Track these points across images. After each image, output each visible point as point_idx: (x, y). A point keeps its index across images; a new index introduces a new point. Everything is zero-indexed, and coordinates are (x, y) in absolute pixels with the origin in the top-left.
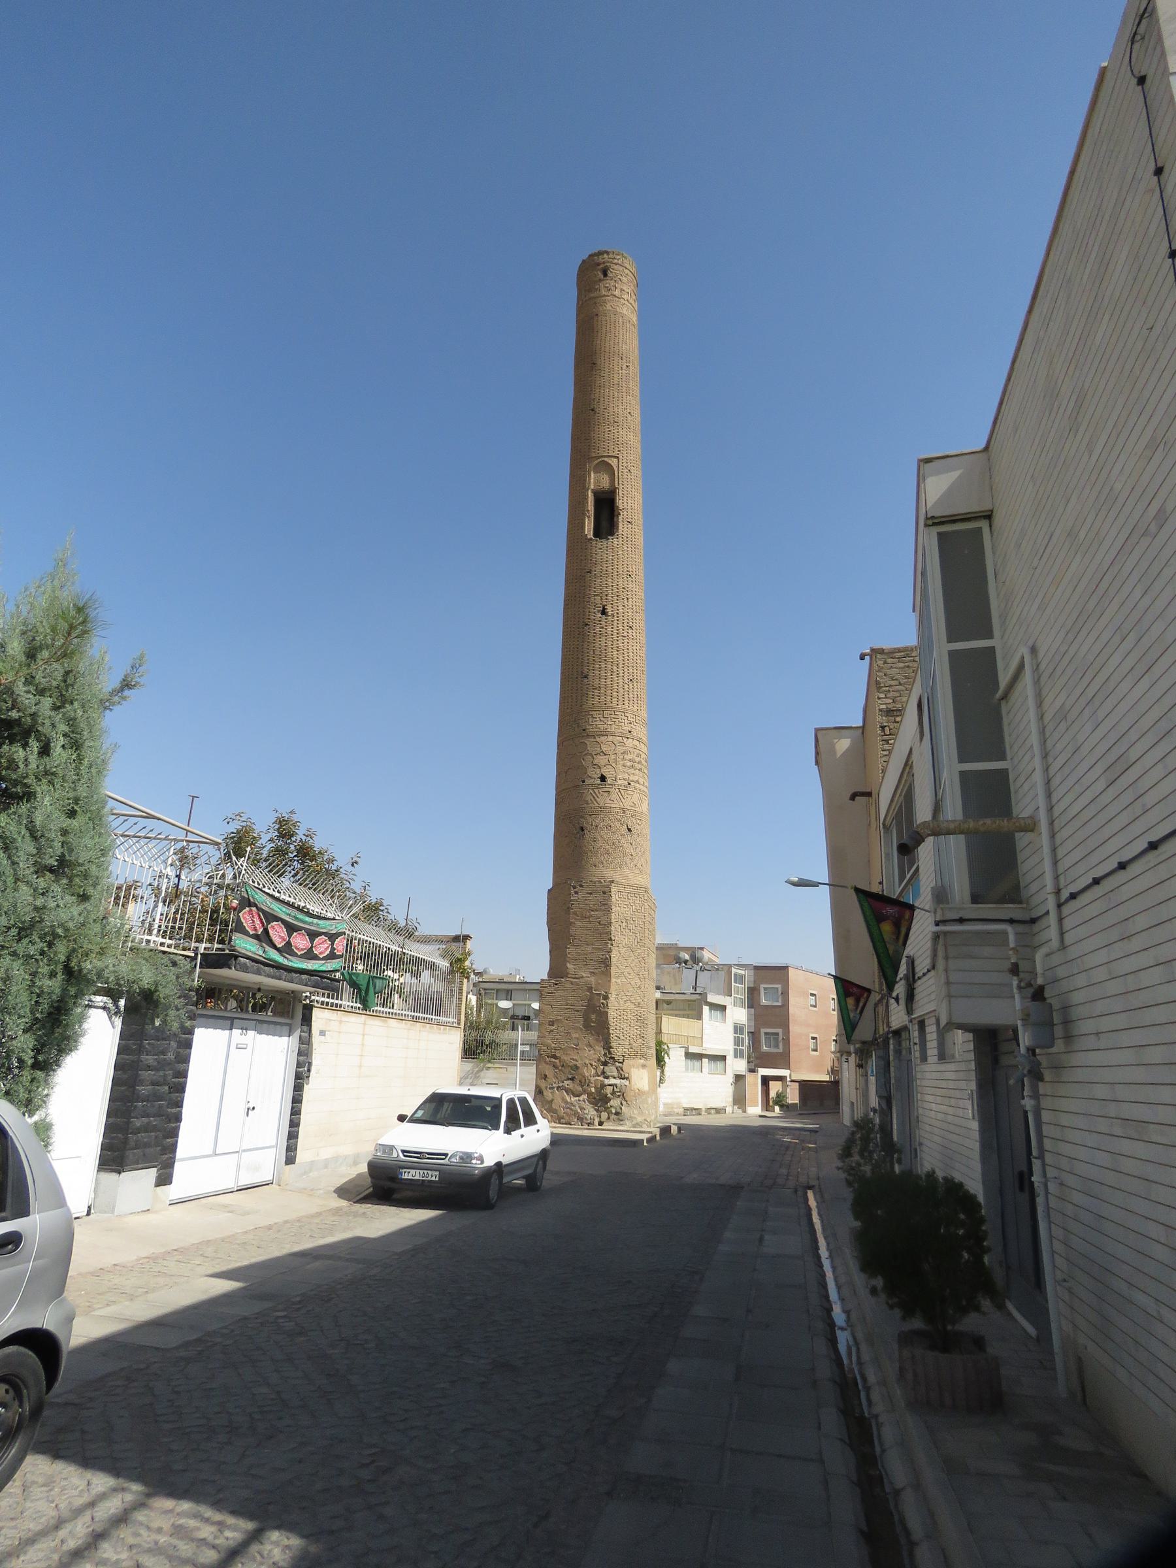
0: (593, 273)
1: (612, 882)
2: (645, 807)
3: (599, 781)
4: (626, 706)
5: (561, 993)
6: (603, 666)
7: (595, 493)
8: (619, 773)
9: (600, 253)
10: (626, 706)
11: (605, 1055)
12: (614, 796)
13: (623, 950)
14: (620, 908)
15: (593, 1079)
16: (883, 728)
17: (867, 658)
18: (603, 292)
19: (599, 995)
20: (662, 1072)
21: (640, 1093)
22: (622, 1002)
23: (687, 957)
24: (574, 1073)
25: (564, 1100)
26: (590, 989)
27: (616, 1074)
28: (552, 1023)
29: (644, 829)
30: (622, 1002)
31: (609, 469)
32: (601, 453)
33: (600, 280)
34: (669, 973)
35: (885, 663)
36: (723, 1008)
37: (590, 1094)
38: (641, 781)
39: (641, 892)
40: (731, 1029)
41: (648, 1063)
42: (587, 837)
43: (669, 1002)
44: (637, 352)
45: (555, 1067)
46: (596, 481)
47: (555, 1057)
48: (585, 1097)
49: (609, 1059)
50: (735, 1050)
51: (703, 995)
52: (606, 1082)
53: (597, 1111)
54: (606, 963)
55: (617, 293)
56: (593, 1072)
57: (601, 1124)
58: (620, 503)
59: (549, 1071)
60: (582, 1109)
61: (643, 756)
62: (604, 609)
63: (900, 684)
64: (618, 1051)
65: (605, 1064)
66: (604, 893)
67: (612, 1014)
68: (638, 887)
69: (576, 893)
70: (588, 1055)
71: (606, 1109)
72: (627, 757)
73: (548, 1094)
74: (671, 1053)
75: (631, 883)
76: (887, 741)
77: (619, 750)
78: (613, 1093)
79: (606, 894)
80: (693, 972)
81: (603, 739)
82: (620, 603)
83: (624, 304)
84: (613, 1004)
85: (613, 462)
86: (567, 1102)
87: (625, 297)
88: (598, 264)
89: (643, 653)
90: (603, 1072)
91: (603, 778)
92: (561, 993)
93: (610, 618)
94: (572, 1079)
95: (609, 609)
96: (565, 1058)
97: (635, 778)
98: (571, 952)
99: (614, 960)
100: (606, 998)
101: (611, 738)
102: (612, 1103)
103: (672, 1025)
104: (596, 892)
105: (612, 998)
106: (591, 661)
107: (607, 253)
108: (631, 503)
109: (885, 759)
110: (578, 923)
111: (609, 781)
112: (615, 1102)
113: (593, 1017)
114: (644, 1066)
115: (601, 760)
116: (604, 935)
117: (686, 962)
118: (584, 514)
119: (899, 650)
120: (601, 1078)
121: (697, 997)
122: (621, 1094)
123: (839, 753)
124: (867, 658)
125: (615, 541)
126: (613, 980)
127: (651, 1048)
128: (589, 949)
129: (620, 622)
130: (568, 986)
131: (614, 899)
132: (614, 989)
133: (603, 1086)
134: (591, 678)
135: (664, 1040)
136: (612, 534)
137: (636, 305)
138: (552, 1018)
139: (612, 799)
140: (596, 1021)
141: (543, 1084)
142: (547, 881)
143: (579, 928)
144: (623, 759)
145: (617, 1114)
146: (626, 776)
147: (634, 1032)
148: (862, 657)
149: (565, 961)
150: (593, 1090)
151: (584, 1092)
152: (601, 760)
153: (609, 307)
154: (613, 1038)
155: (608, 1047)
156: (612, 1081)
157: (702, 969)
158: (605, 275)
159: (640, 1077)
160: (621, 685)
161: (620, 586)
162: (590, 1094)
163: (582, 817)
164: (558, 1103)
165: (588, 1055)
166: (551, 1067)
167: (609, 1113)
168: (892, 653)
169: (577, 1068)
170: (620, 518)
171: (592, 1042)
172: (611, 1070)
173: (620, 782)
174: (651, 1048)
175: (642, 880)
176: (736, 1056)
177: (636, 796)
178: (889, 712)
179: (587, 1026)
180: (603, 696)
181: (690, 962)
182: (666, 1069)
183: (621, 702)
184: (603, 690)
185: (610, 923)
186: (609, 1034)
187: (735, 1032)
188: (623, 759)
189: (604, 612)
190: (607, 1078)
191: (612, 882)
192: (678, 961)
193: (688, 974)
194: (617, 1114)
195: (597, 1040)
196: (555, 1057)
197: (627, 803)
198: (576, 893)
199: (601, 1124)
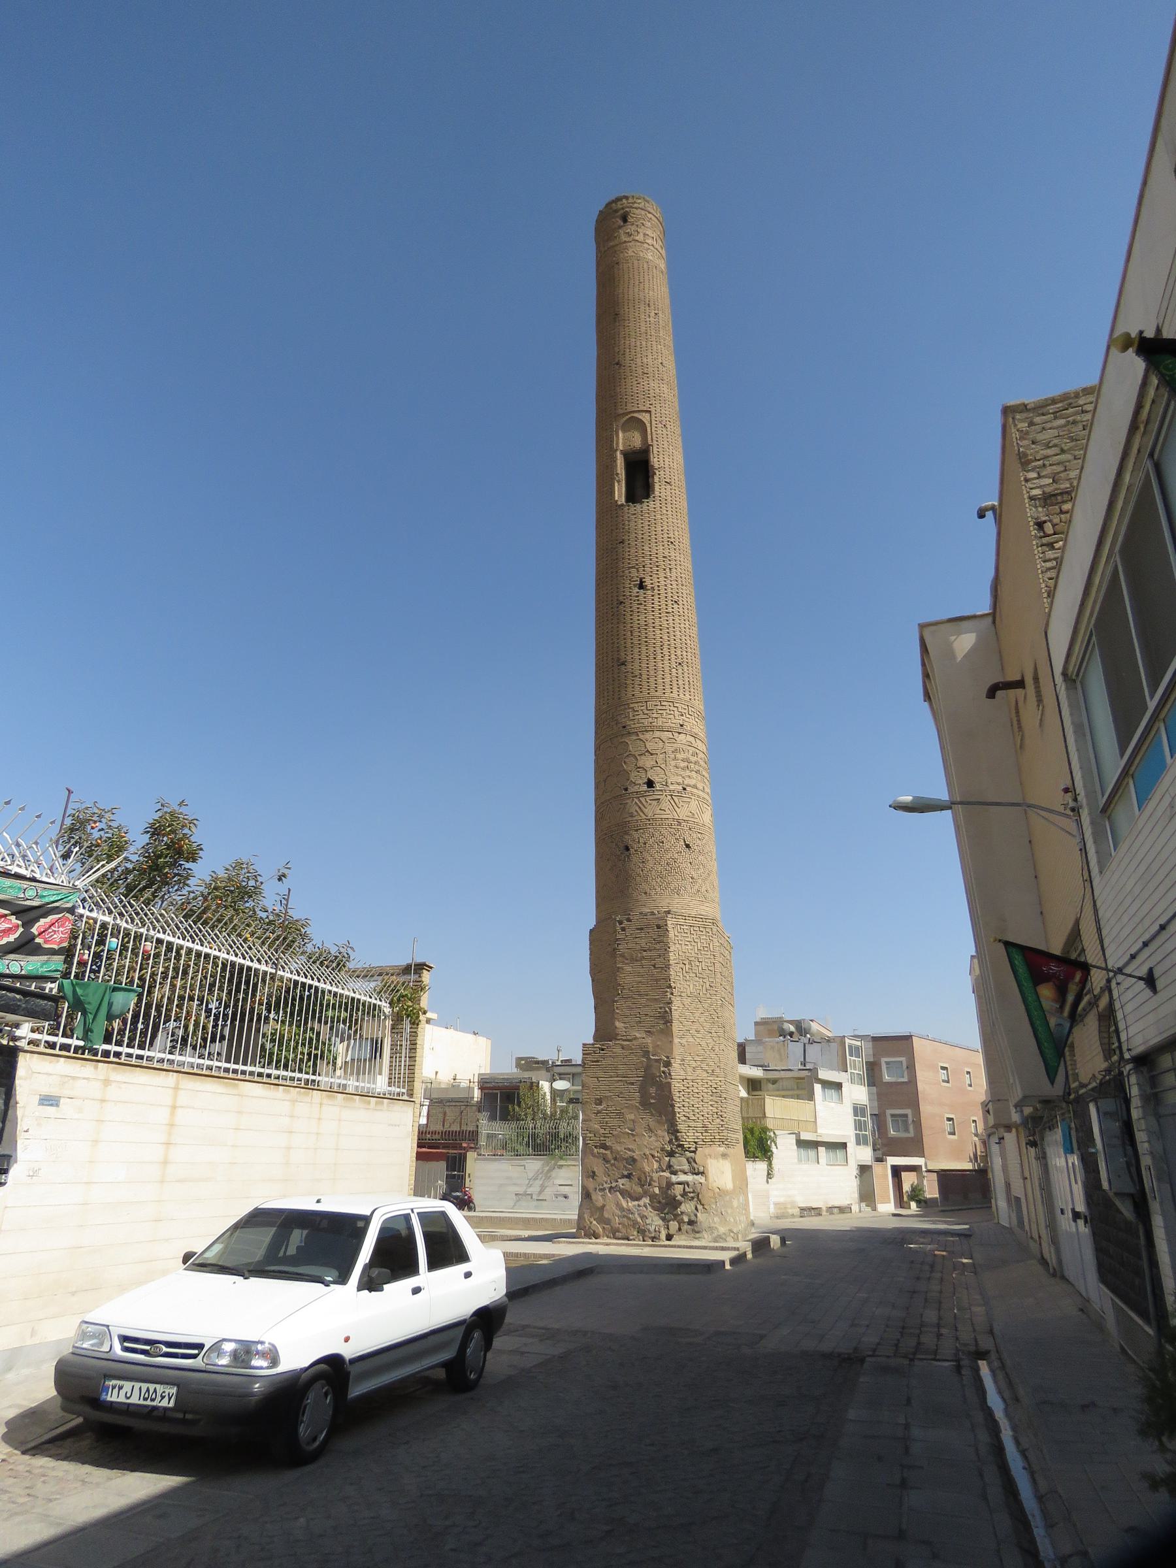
0: (613, 221)
1: (669, 912)
2: (707, 818)
3: (645, 788)
4: (675, 695)
5: (609, 1061)
6: (644, 648)
7: (626, 455)
8: (670, 776)
9: (618, 199)
10: (675, 695)
11: (670, 1142)
12: (665, 804)
13: (687, 1001)
14: (680, 944)
15: (655, 1176)
16: (1040, 525)
17: (989, 514)
18: (624, 238)
19: (657, 1061)
20: (770, 1165)
21: (722, 1192)
22: (689, 1070)
23: (792, 1028)
24: (629, 1167)
25: (618, 1205)
26: (646, 1053)
27: (686, 1167)
28: (599, 1102)
29: (708, 844)
30: (689, 1070)
31: (641, 427)
32: (630, 408)
33: (620, 227)
34: (772, 1048)
35: (1031, 424)
36: (838, 1086)
37: (653, 1197)
38: (700, 786)
39: (705, 923)
40: (851, 1111)
41: (730, 1151)
42: (635, 859)
43: (774, 1082)
44: (667, 301)
45: (606, 1160)
46: (624, 440)
47: (604, 1146)
48: (646, 1200)
49: (676, 1147)
50: (857, 1136)
51: (814, 1071)
52: (674, 1178)
53: (663, 1219)
54: (666, 1019)
55: (640, 237)
56: (656, 1165)
57: (669, 1237)
58: (655, 461)
59: (599, 1168)
60: (643, 1217)
61: (701, 755)
62: (642, 582)
63: (1063, 451)
64: (688, 1136)
65: (671, 1154)
66: (659, 927)
67: (676, 1086)
68: (703, 918)
69: (623, 929)
70: (648, 1143)
71: (676, 1216)
72: (680, 756)
73: (598, 1198)
74: (778, 1141)
75: (693, 913)
76: (1051, 546)
77: (669, 748)
78: (684, 1194)
79: (661, 927)
80: (800, 1046)
81: (648, 736)
82: (662, 574)
83: (649, 248)
84: (680, 1075)
85: (645, 418)
86: (622, 1209)
87: (650, 241)
88: (616, 211)
89: (694, 631)
90: (669, 1166)
91: (650, 784)
92: (609, 1061)
93: (649, 592)
94: (629, 1176)
95: (648, 582)
96: (618, 1148)
97: (693, 782)
98: (621, 1006)
99: (675, 1014)
100: (668, 1064)
101: (657, 734)
102: (683, 1208)
103: (776, 1108)
104: (648, 926)
105: (676, 1065)
106: (629, 645)
107: (627, 198)
108: (669, 461)
109: (1052, 574)
110: (628, 968)
111: (658, 786)
112: (687, 1207)
113: (652, 1090)
114: (724, 1156)
115: (646, 761)
116: (661, 983)
117: (791, 1034)
118: (613, 479)
119: (1054, 401)
120: (667, 1174)
121: (806, 1073)
122: (694, 1195)
123: (960, 655)
124: (989, 514)
125: (649, 505)
126: (676, 1040)
127: (735, 1131)
128: (643, 1001)
129: (663, 596)
130: (618, 1050)
131: (671, 934)
132: (677, 1051)
133: (670, 1185)
134: (629, 666)
135: (770, 1126)
136: (648, 497)
137: (663, 252)
138: (598, 1095)
139: (663, 809)
140: (657, 1098)
141: (591, 1185)
142: (589, 919)
143: (629, 975)
144: (675, 759)
145: (691, 1223)
146: (680, 780)
147: (707, 1109)
148: (981, 515)
149: (613, 1019)
150: (657, 1190)
151: (645, 1194)
152: (646, 761)
153: (630, 253)
154: (680, 1118)
155: (674, 1131)
156: (682, 1178)
157: (811, 1042)
158: (625, 220)
159: (721, 1170)
160: (667, 669)
161: (660, 556)
162: (653, 1197)
163: (626, 833)
164: (611, 1211)
165: (648, 1143)
166: (601, 1161)
167: (681, 1222)
168: (1040, 408)
169: (634, 1160)
170: (656, 479)
171: (652, 1124)
172: (680, 1162)
173: (672, 787)
174: (735, 1131)
175: (710, 909)
176: (858, 1143)
177: (694, 804)
178: (1048, 499)
179: (645, 1103)
180: (645, 684)
181: (796, 1034)
182: (775, 1161)
183: (668, 691)
184: (644, 677)
185: (668, 966)
186: (674, 1113)
187: (856, 1114)
188: (675, 759)
189: (641, 586)
190: (675, 1173)
191: (669, 912)
192: (783, 1033)
193: (795, 1049)
194: (691, 1223)
195: (659, 1122)
196: (604, 1146)
197: (683, 813)
198: (623, 929)
199: (669, 1237)
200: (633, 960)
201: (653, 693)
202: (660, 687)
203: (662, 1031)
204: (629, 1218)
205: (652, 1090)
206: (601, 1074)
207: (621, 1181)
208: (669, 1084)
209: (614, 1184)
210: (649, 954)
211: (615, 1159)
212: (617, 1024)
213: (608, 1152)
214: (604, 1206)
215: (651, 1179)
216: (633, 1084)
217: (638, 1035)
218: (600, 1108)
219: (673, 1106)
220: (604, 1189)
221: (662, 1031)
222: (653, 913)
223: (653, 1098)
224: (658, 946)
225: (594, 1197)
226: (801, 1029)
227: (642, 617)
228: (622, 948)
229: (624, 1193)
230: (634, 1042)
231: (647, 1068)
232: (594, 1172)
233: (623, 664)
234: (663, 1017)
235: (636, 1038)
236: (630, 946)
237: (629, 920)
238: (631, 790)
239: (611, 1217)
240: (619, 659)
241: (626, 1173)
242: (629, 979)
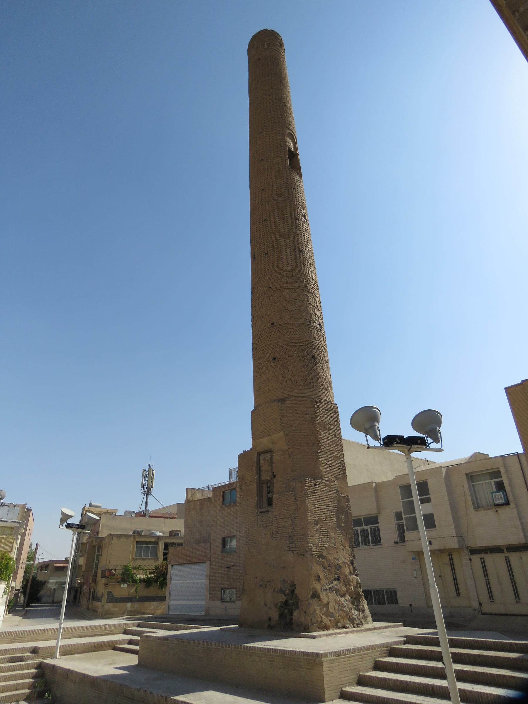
25: (335, 600)
86: (339, 604)
94: (338, 579)
113: (343, 517)
130: (323, 486)
169: (340, 567)
179: (339, 526)
200: (325, 429)
204: (344, 611)
205: (343, 517)
207: (335, 583)
209: (331, 585)
211: (329, 566)
212: (321, 468)
213: (325, 561)
214: (328, 603)
215: (350, 581)
216: (331, 512)
218: (318, 527)
220: (326, 590)
225: (321, 596)
229: (337, 591)
231: (339, 502)
232: (319, 577)
235: (331, 480)
236: (323, 419)
237: (320, 402)
239: (334, 611)
241: (336, 576)
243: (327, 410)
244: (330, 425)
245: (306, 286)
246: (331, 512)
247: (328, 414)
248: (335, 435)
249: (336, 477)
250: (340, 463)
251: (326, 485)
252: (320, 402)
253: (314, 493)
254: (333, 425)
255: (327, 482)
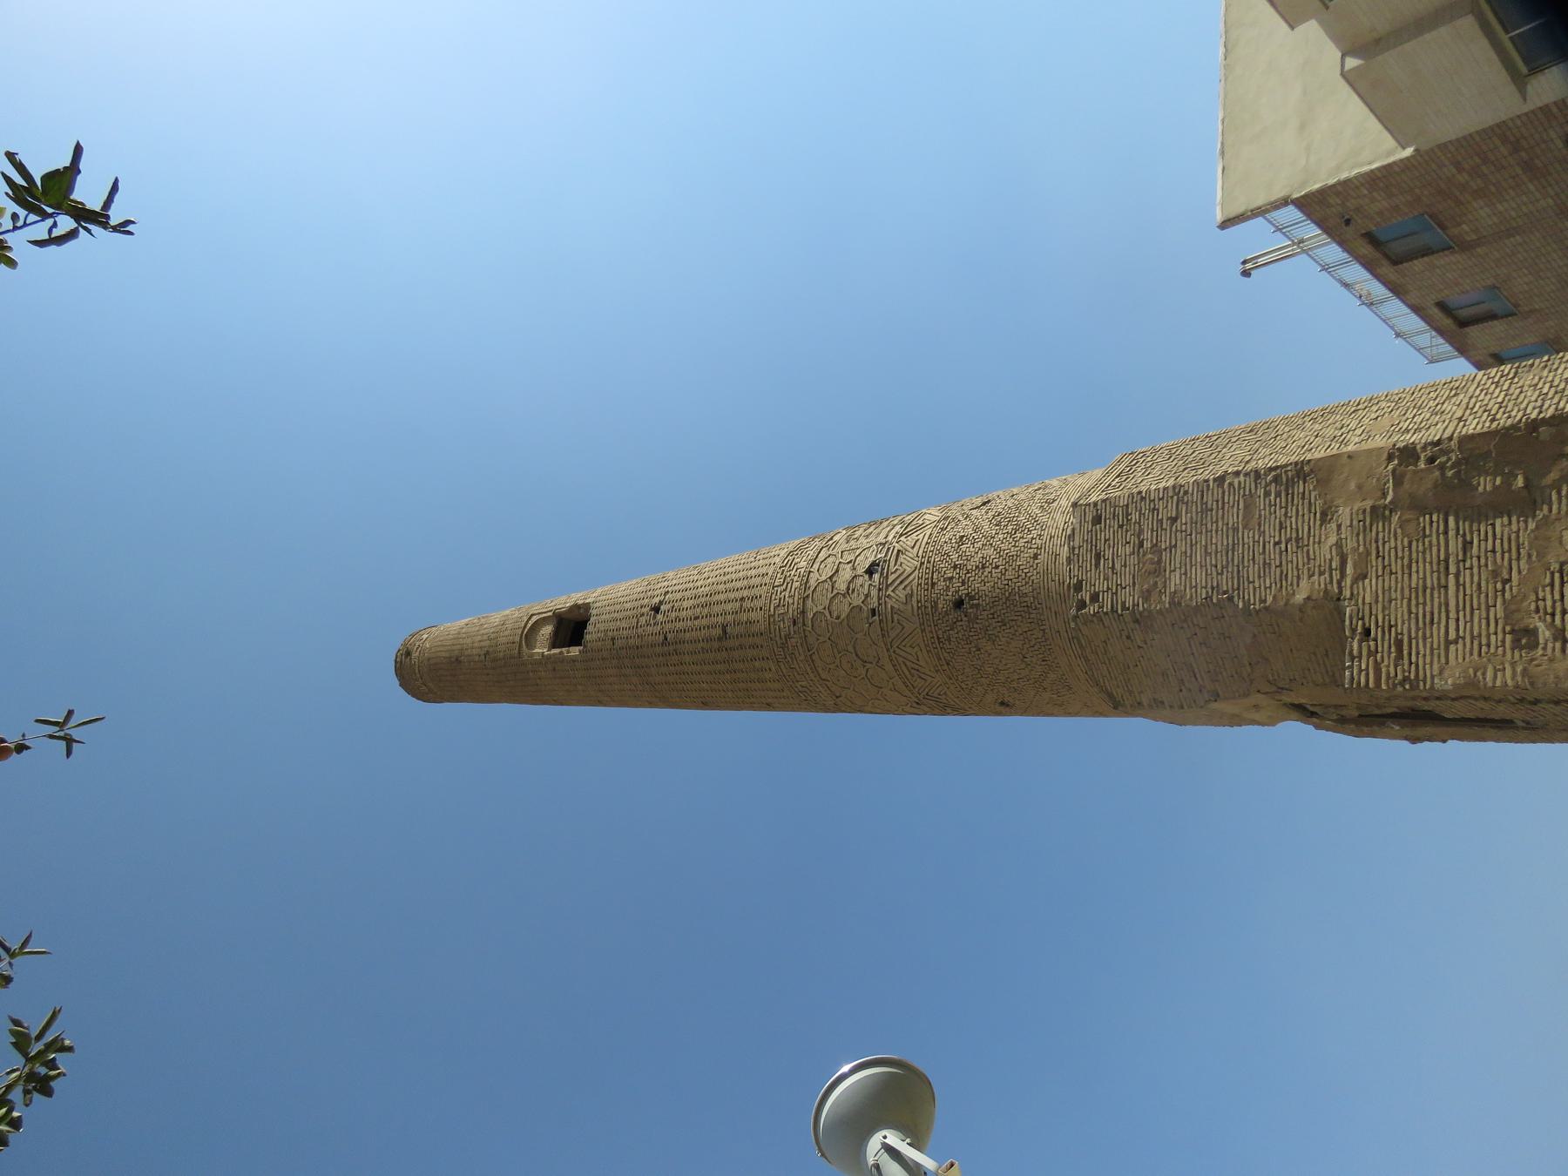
5: (1399, 612)
6: (717, 597)
19: (1398, 482)
26: (1377, 513)
66: (1097, 520)
69: (1095, 598)
92: (1399, 612)
95: (657, 600)
100: (1407, 454)
110: (1175, 580)
113: (1485, 484)
130: (1368, 589)
138: (1499, 638)
152: (846, 574)
179: (1528, 503)
180: (755, 592)
184: (745, 593)
189: (656, 609)
200: (1158, 570)
201: (767, 580)
202: (763, 571)
203: (1323, 483)
205: (1485, 484)
206: (1437, 634)
208: (1466, 440)
210: (1147, 535)
212: (1300, 597)
216: (1467, 545)
217: (1333, 539)
218: (1544, 633)
219: (1534, 425)
221: (1323, 483)
222: (1071, 537)
223: (1507, 483)
224: (1135, 517)
226: (1398, 335)
227: (685, 604)
228: (1129, 597)
230: (1350, 544)
231: (1420, 507)
233: (724, 628)
234: (1290, 483)
235: (1339, 545)
236: (1128, 580)
237: (1078, 587)
238: (874, 603)
240: (720, 639)
242: (1199, 576)
243: (1098, 556)
244: (1141, 545)
245: (794, 623)
246: (1467, 545)
247: (1109, 554)
248: (1174, 520)
249: (1324, 514)
250: (1267, 494)
251: (1361, 576)
252: (1078, 587)
253: (1399, 644)
254: (1141, 531)
255: (1349, 570)
